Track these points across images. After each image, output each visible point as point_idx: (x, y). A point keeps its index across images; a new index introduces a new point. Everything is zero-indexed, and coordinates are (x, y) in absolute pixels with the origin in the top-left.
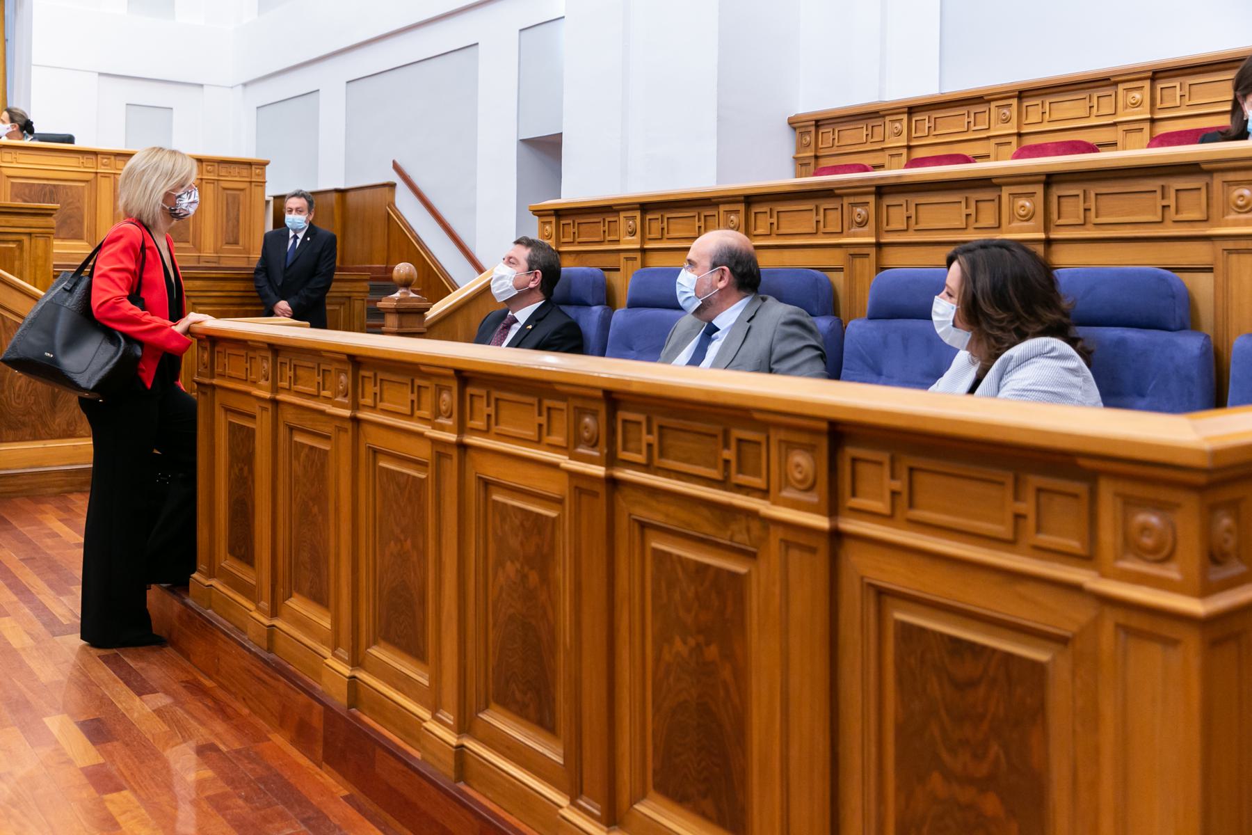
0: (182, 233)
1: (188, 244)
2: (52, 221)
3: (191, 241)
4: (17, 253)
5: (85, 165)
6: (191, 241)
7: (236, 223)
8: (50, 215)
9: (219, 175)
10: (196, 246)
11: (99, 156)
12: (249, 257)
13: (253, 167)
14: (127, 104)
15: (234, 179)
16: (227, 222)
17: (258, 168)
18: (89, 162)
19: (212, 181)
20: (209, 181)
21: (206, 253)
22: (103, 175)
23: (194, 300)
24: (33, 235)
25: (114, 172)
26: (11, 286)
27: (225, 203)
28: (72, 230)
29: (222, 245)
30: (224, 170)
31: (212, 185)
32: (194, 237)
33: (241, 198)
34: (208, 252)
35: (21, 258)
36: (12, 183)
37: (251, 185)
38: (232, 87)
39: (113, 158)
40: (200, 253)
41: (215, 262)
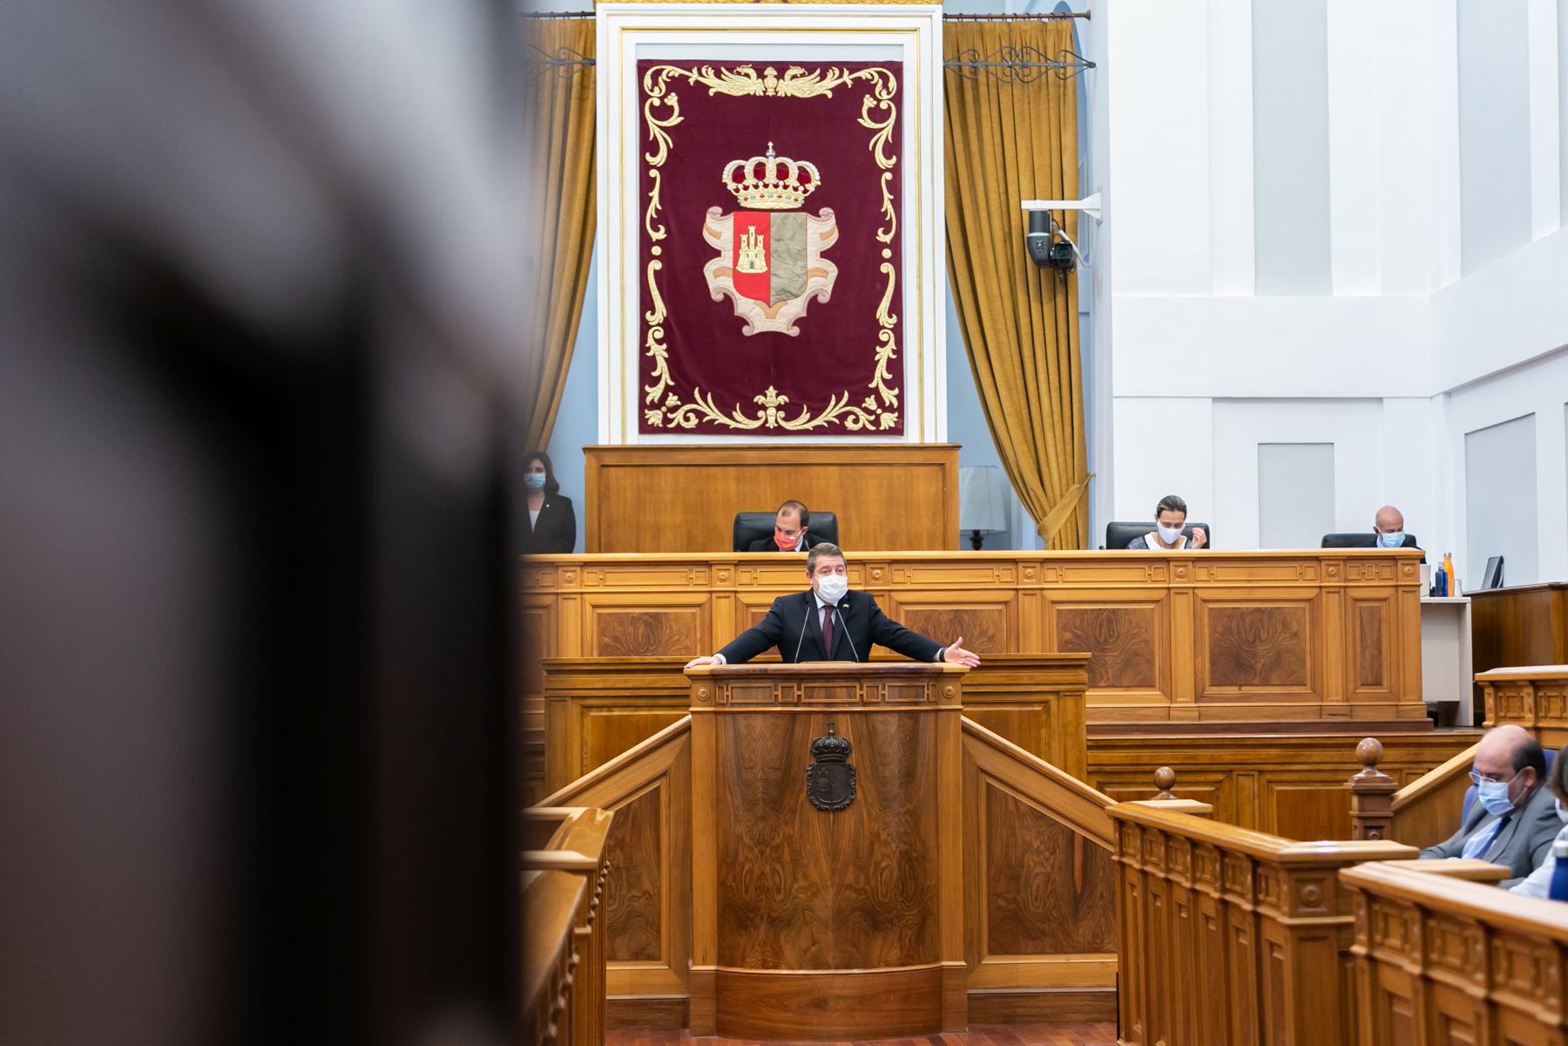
0: (1295, 672)
1: (1304, 687)
2: (1083, 675)
3: (1309, 683)
4: (1044, 718)
5: (1154, 579)
6: (1309, 683)
7: (1375, 652)
8: (1081, 667)
9: (1346, 580)
10: (1318, 693)
11: (1172, 564)
12: (1397, 705)
13: (1400, 563)
14: (1259, 444)
15: (1367, 585)
16: (1363, 650)
17: (1408, 564)
18: (1159, 573)
19: (1337, 590)
20: (1332, 590)
21: (1332, 701)
22: (1177, 591)
23: (1269, 777)
24: (1061, 694)
25: (1193, 585)
26: (1024, 764)
27: (1358, 622)
28: (1140, 674)
29: (1355, 689)
30: (1354, 571)
31: (1337, 595)
32: (1313, 679)
33: (1384, 612)
34: (1334, 701)
35: (1048, 724)
36: (1058, 610)
37: (1397, 591)
38: (1431, 397)
39: (1190, 564)
40: (1323, 701)
41: (1344, 715)
